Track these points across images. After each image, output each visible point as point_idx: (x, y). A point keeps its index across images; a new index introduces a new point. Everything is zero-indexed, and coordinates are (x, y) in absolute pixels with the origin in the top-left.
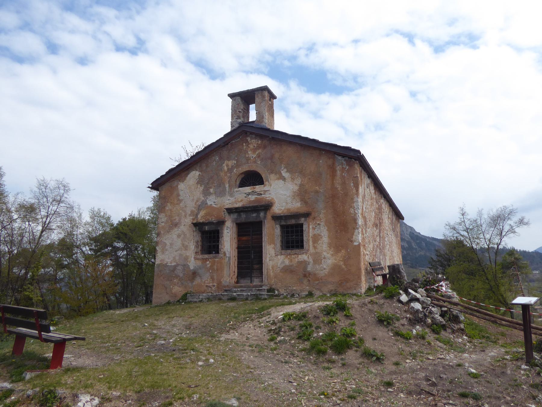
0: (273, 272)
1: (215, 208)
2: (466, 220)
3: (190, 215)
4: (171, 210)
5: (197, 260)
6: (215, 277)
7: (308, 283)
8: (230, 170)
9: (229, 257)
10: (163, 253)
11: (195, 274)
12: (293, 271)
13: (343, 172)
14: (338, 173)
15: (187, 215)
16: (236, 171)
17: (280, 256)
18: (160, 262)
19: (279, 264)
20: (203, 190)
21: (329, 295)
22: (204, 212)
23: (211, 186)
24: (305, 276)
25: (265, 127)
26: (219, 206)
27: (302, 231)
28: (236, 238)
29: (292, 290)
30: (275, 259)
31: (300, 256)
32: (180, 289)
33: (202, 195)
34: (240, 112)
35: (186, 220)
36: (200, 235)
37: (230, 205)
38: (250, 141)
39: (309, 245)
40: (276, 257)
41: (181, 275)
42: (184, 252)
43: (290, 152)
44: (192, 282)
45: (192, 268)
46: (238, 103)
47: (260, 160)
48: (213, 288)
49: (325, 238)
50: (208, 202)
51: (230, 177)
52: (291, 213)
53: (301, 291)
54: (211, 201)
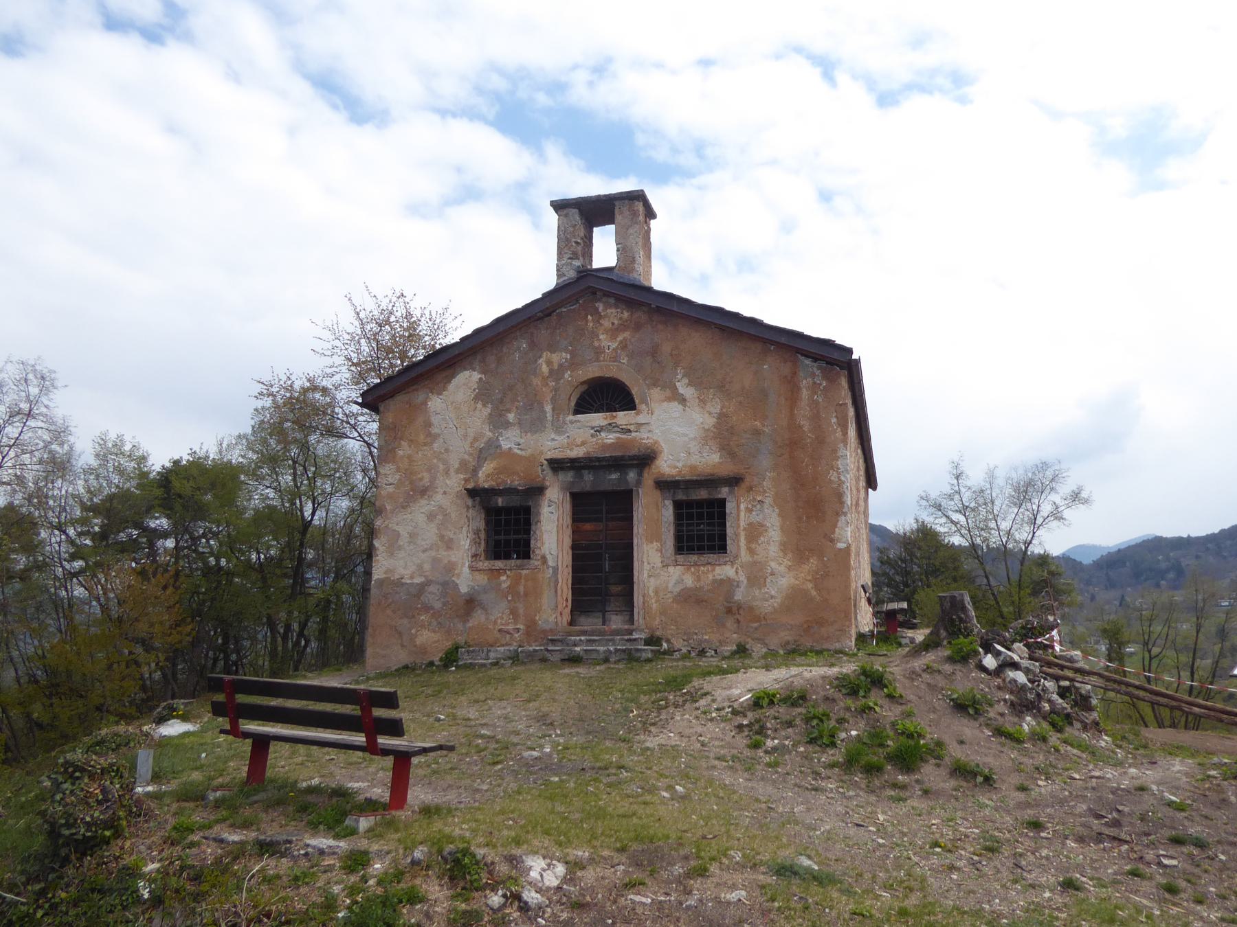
1: (521, 456)
2: (963, 490)
3: (458, 471)
4: (409, 457)
5: (477, 573)
6: (521, 611)
7: (735, 625)
8: (556, 374)
9: (553, 568)
10: (391, 554)
11: (471, 603)
12: (702, 601)
13: (816, 393)
14: (805, 393)
15: (452, 470)
16: (570, 376)
18: (384, 576)
19: (670, 585)
20: (490, 414)
21: (781, 652)
22: (492, 465)
23: (508, 406)
24: (729, 611)
25: (638, 284)
26: (529, 452)
27: (723, 515)
28: (570, 527)
29: (701, 642)
30: (662, 573)
31: (717, 568)
32: (436, 637)
33: (487, 427)
34: (577, 243)
35: (448, 482)
36: (483, 516)
37: (557, 451)
38: (603, 310)
39: (739, 546)
41: (438, 605)
42: (444, 553)
43: (695, 340)
44: (467, 621)
45: (464, 589)
46: (574, 222)
47: (627, 356)
48: (517, 635)
49: (773, 533)
50: (502, 443)
51: (556, 390)
52: (699, 475)
53: (721, 643)
54: (510, 440)
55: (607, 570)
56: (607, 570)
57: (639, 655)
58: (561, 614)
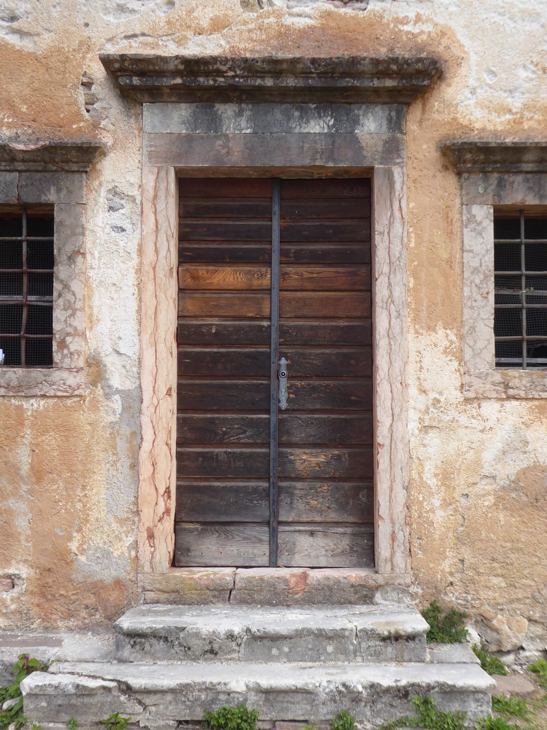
0: (446, 504)
9: (125, 395)
17: (496, 405)
19: (488, 456)
30: (463, 419)
40: (472, 409)
55: (284, 405)
56: (284, 405)
57: (454, 707)
58: (151, 536)
